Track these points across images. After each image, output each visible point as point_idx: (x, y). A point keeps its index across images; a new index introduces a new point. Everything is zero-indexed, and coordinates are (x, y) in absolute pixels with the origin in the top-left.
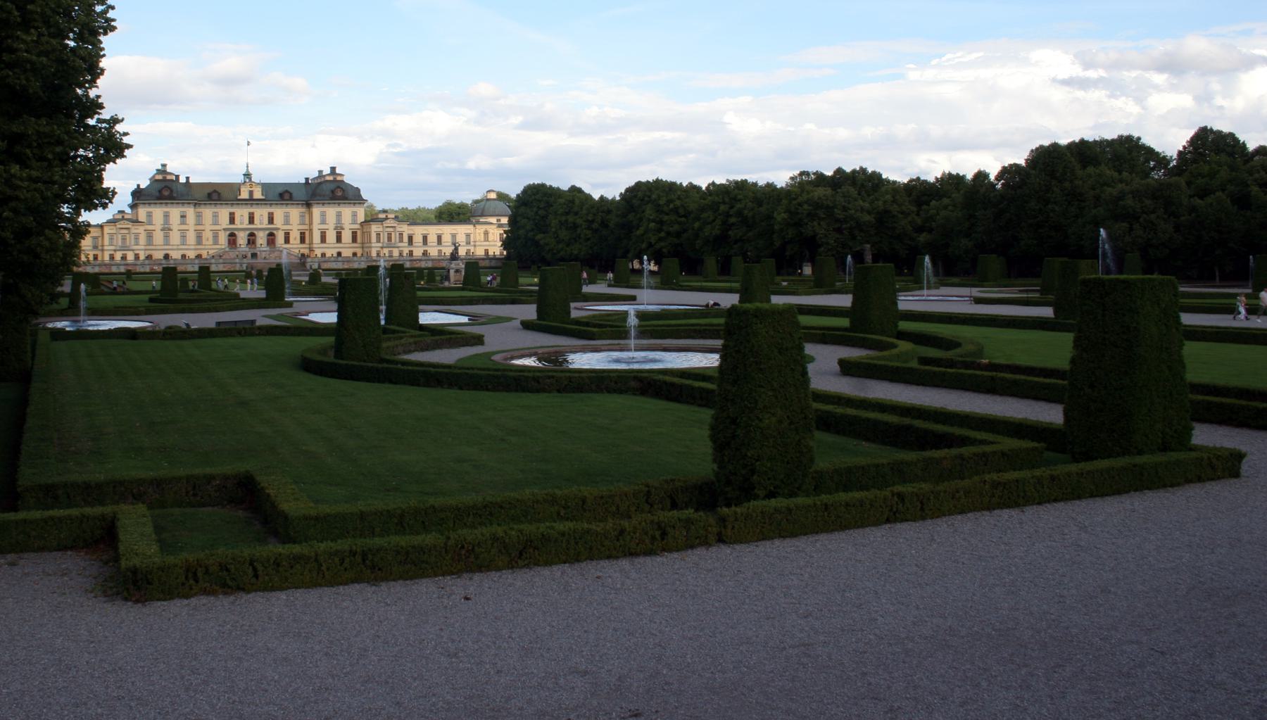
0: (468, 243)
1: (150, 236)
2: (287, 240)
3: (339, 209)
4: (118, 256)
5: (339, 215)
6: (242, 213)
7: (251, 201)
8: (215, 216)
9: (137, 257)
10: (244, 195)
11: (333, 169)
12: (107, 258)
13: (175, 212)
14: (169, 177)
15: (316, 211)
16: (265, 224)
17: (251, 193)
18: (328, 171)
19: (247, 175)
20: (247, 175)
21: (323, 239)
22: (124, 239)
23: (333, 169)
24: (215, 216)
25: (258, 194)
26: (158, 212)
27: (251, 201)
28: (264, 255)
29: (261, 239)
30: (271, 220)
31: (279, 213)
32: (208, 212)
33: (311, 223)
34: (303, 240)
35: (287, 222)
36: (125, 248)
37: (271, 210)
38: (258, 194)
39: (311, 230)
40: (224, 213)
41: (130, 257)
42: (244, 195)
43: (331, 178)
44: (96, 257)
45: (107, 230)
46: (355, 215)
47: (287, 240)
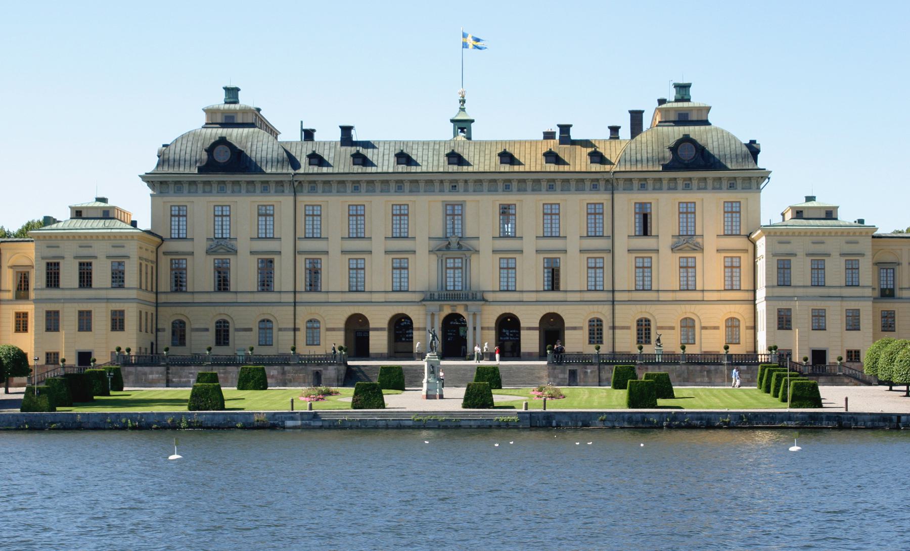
5: (687, 212)
13: (243, 207)
15: (625, 204)
26: (201, 207)
46: (732, 211)
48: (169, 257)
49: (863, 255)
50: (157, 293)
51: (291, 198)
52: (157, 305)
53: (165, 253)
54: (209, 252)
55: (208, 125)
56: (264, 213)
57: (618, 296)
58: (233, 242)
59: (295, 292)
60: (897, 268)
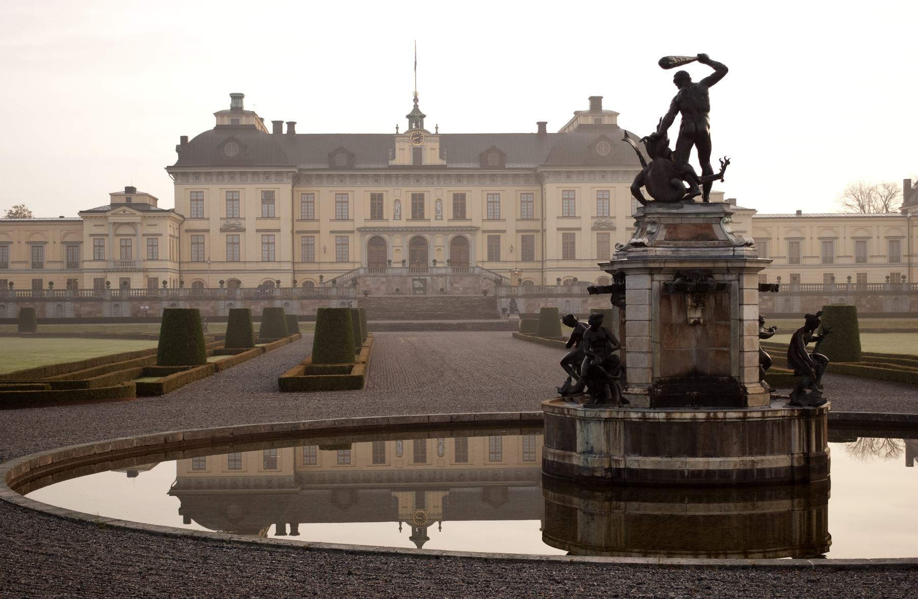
0: (894, 259)
1: (198, 237)
2: (494, 254)
3: (603, 186)
4: (114, 281)
6: (398, 197)
7: (417, 171)
8: (342, 202)
9: (153, 282)
10: (403, 157)
11: (596, 102)
12: (87, 283)
13: (250, 193)
14: (244, 121)
15: (553, 190)
16: (447, 219)
17: (417, 154)
18: (586, 106)
19: (416, 117)
20: (416, 117)
21: (569, 251)
22: (126, 247)
23: (596, 102)
24: (342, 202)
25: (432, 157)
26: (214, 194)
27: (417, 171)
28: (440, 283)
29: (439, 251)
30: (460, 208)
31: (476, 197)
32: (325, 196)
33: (543, 219)
34: (527, 254)
35: (494, 216)
36: (126, 265)
37: (459, 189)
38: (432, 157)
39: (544, 231)
40: (359, 197)
41: (138, 282)
42: (403, 157)
43: (590, 121)
44: (72, 284)
45: (89, 228)
47: (494, 254)
48: (190, 234)
49: (745, 232)
50: (180, 263)
51: (289, 187)
52: (180, 272)
53: (187, 231)
54: (222, 230)
55: (218, 128)
56: (268, 198)
57: (548, 265)
58: (242, 222)
59: (293, 263)
60: (802, 242)
